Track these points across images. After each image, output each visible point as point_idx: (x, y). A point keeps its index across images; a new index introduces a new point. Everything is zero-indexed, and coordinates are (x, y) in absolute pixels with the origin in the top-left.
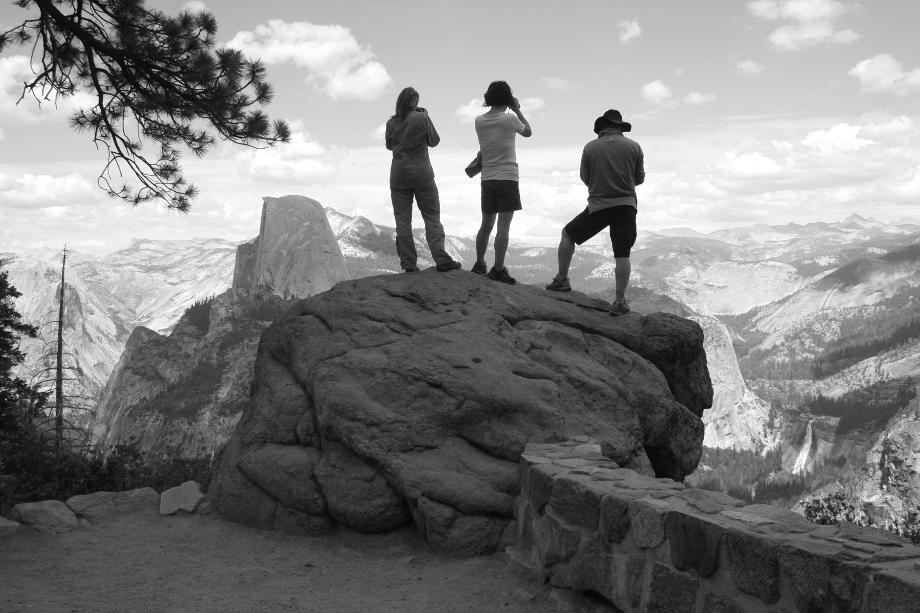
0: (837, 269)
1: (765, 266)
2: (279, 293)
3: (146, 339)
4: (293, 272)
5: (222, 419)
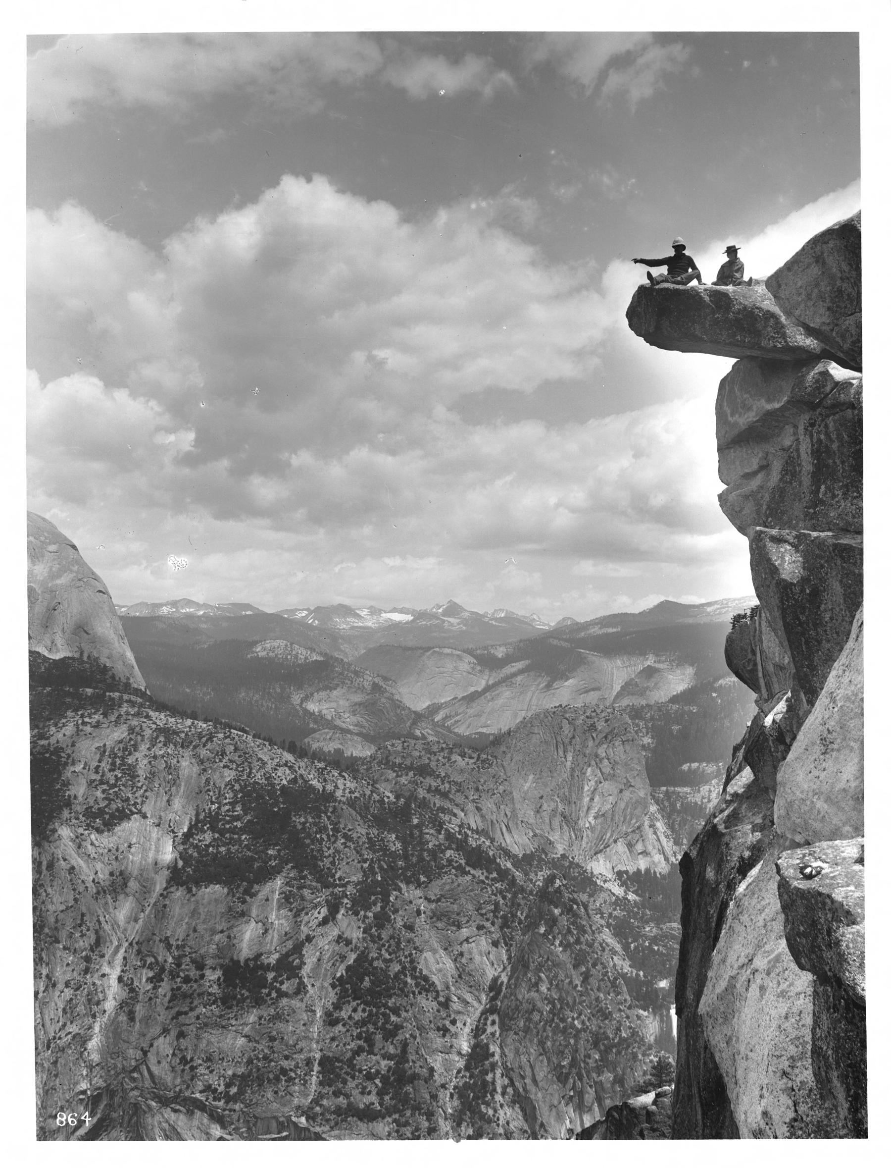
0: (527, 662)
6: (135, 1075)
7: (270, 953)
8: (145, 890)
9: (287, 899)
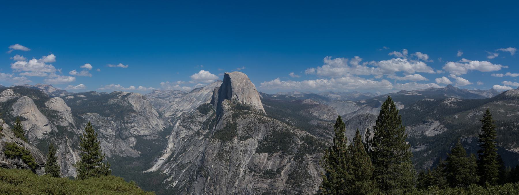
1: (348, 102)
2: (240, 102)
3: (186, 116)
4: (245, 95)
5: (241, 142)
6: (244, 190)
7: (275, 168)
8: (251, 154)
9: (280, 156)
